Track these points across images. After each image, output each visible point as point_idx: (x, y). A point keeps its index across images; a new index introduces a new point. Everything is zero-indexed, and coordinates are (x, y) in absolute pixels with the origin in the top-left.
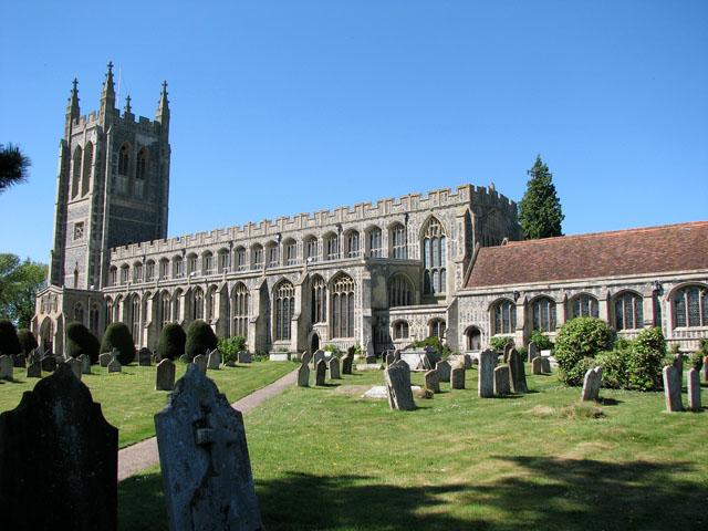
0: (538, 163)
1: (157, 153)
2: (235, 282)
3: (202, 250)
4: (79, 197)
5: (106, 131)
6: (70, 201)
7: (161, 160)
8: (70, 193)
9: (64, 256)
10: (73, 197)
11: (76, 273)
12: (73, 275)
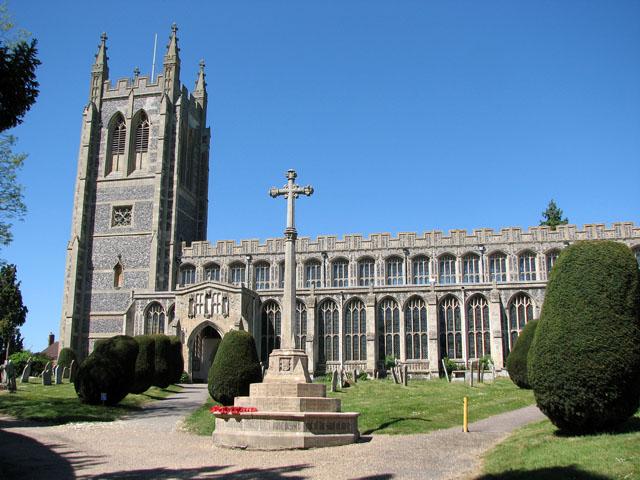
0: (553, 206)
1: (199, 139)
2: (512, 293)
3: (357, 255)
4: (113, 174)
5: (175, 100)
6: (99, 179)
7: (203, 149)
8: (102, 168)
9: (91, 246)
10: (106, 174)
11: (118, 268)
12: (112, 271)
